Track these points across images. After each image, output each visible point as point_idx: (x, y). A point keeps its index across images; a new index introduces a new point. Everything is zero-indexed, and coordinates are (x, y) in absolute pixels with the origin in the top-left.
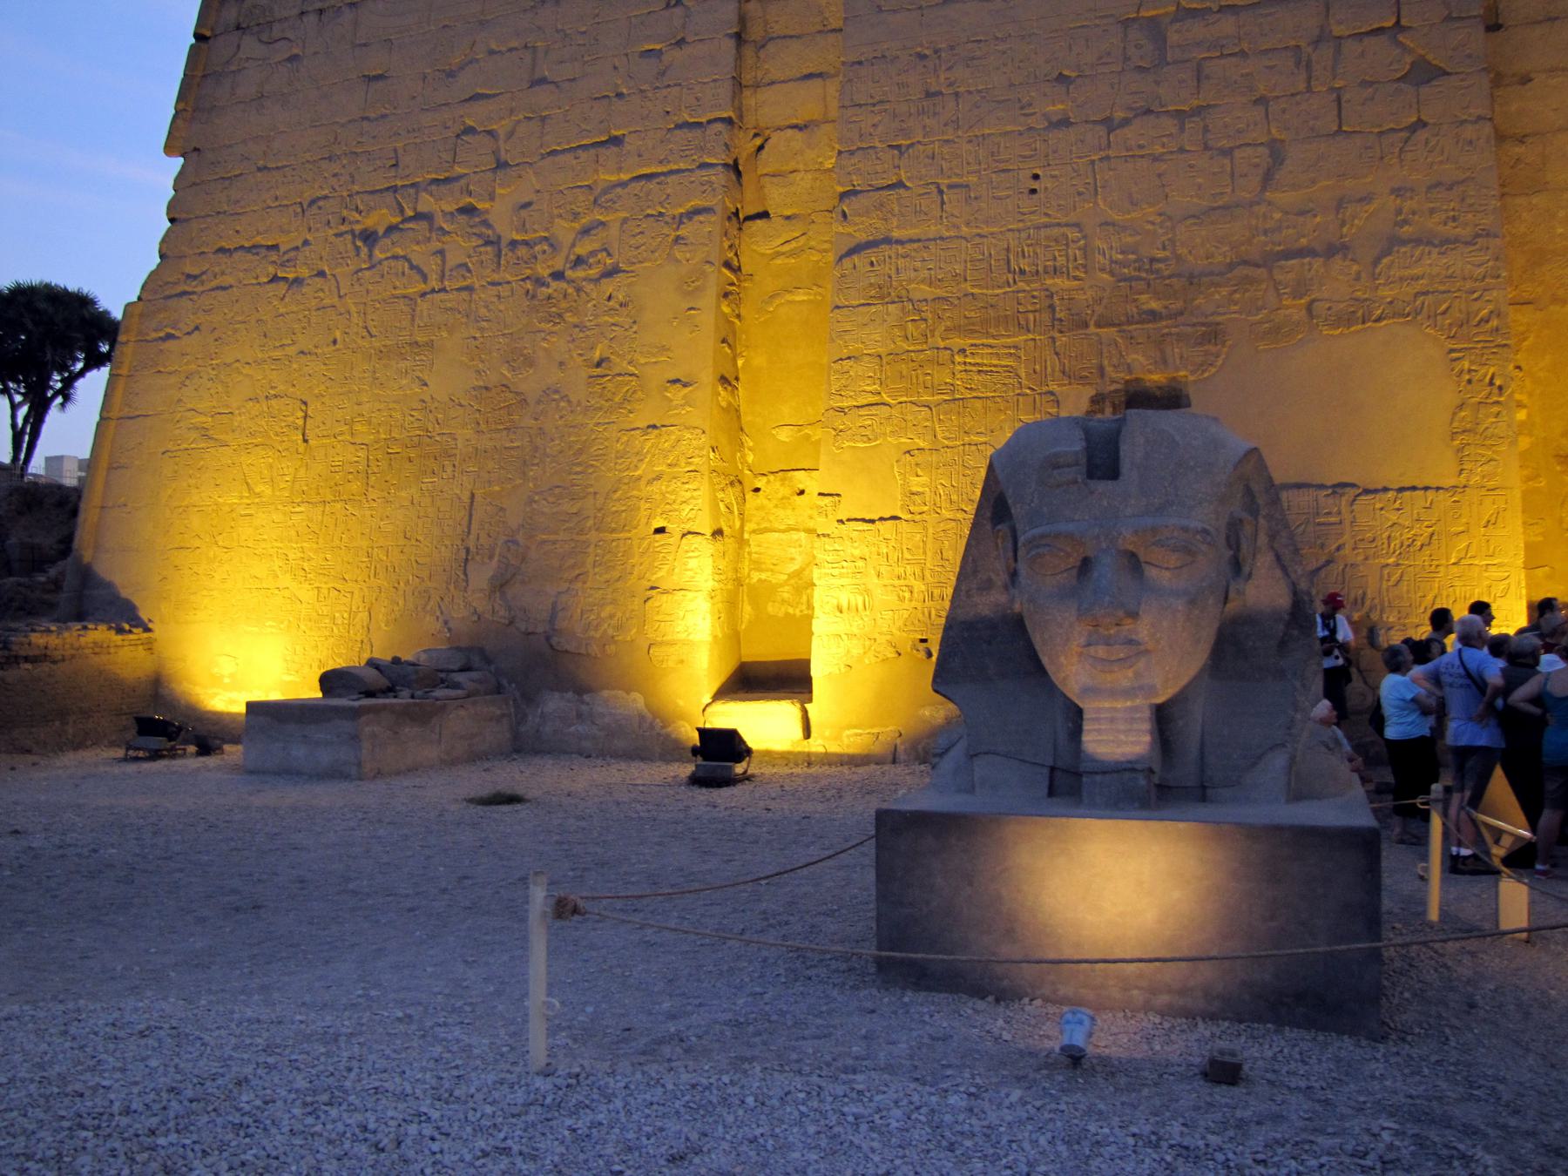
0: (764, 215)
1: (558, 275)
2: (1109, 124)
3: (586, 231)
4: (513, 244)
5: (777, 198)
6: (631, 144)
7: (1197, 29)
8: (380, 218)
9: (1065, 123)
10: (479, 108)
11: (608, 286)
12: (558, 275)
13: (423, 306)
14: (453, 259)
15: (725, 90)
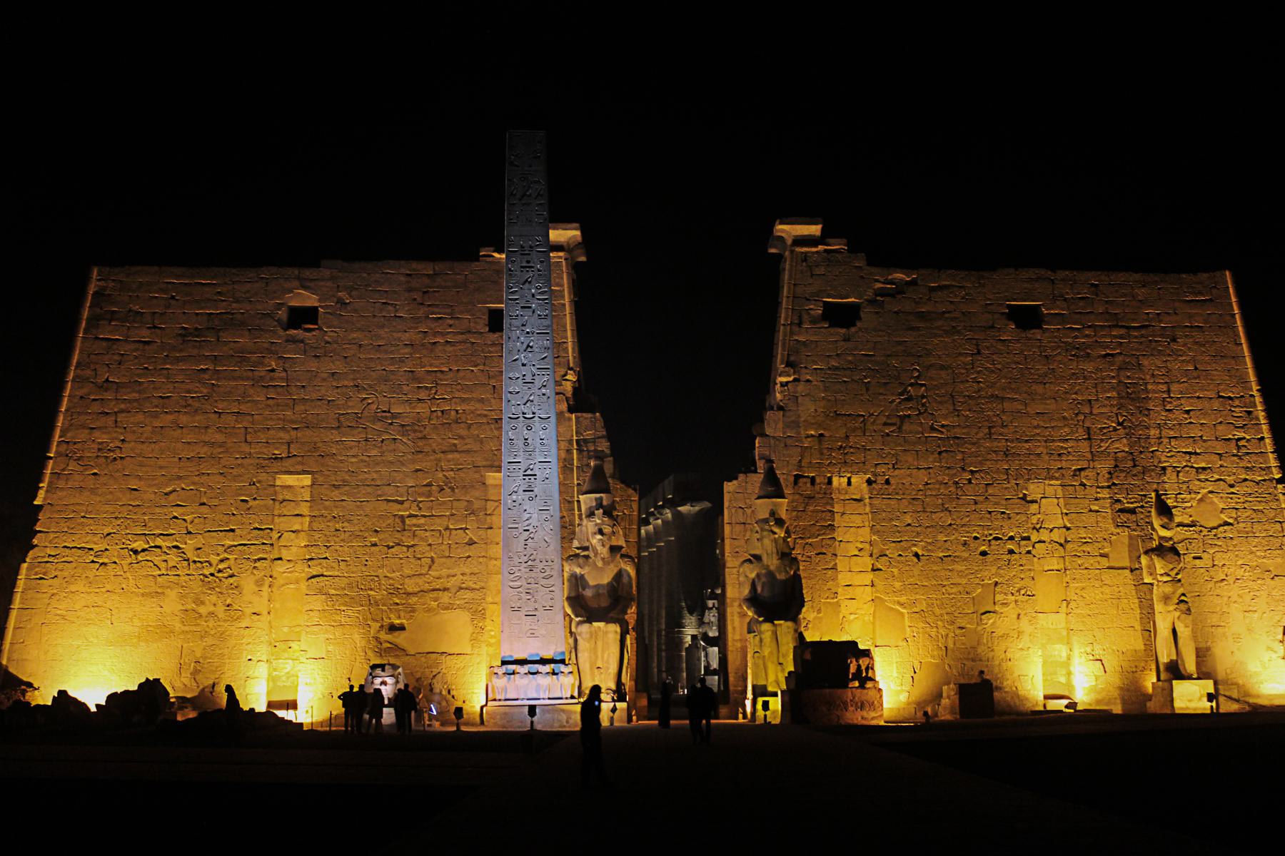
0: (280, 559)
1: (212, 575)
2: (389, 547)
3: (222, 561)
4: (195, 562)
5: (285, 554)
6: (238, 532)
7: (414, 521)
8: (139, 545)
9: (375, 545)
10: (181, 510)
11: (231, 580)
12: (212, 575)
13: (159, 579)
14: (171, 564)
15: (270, 518)
